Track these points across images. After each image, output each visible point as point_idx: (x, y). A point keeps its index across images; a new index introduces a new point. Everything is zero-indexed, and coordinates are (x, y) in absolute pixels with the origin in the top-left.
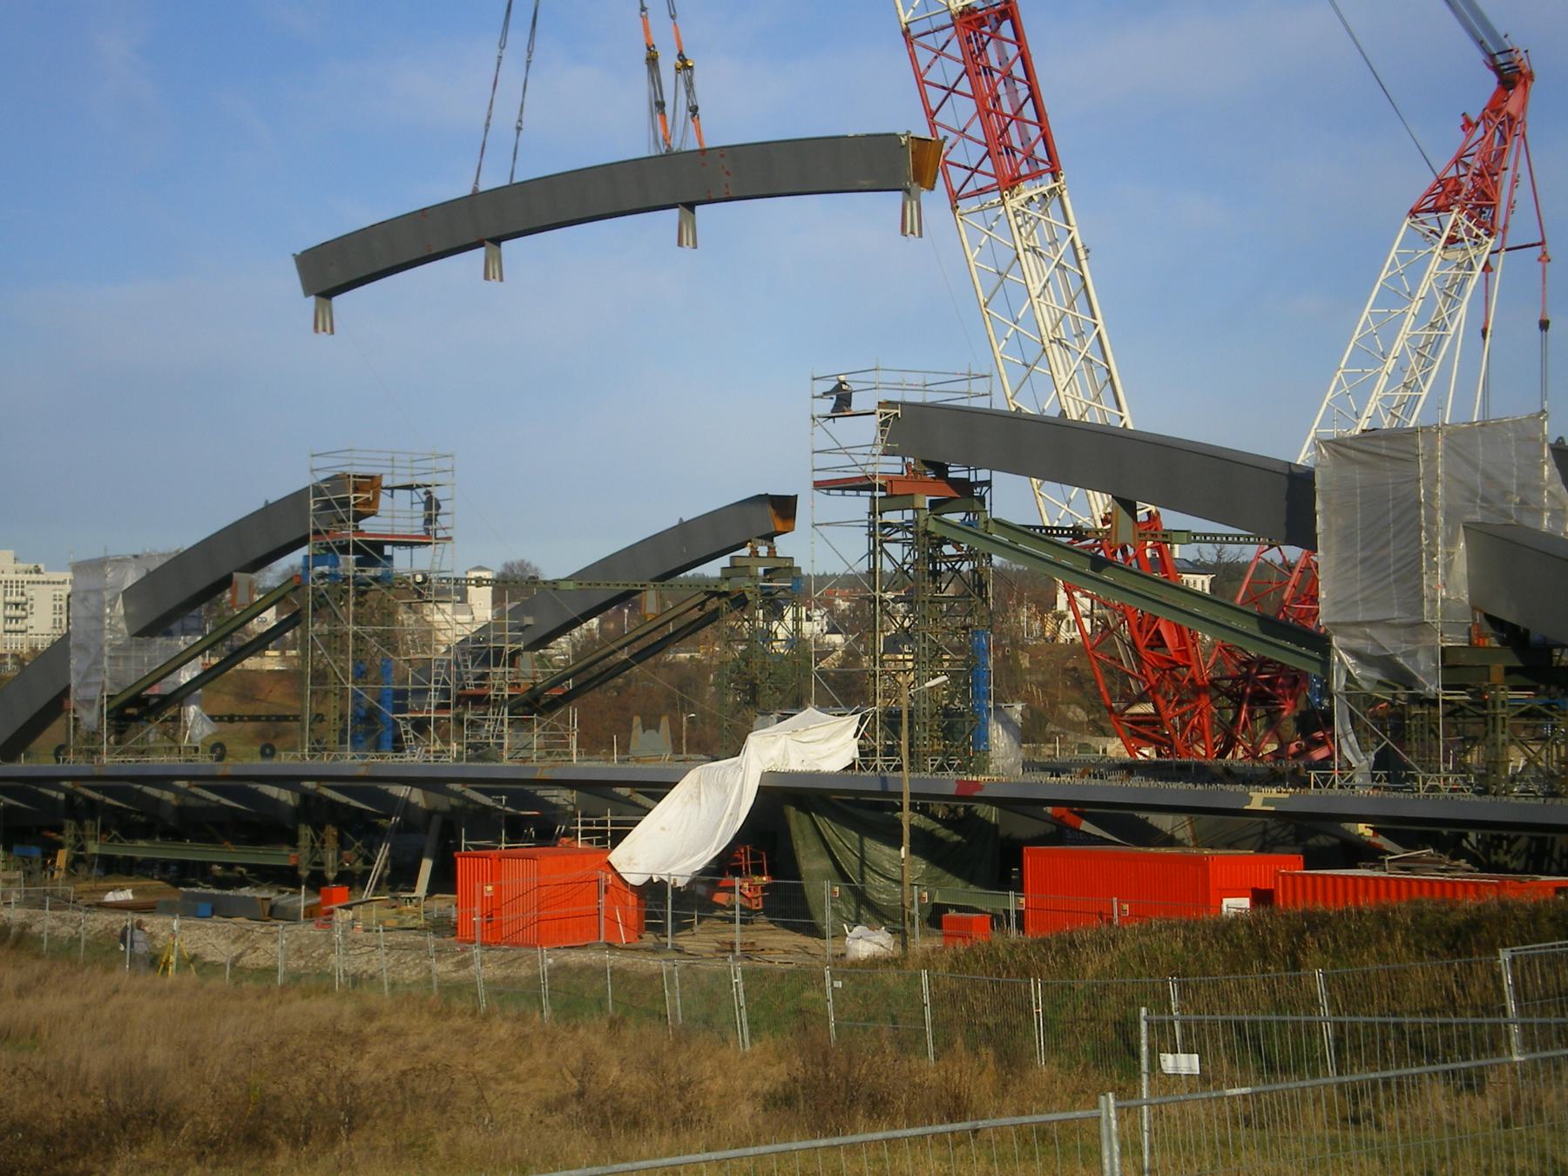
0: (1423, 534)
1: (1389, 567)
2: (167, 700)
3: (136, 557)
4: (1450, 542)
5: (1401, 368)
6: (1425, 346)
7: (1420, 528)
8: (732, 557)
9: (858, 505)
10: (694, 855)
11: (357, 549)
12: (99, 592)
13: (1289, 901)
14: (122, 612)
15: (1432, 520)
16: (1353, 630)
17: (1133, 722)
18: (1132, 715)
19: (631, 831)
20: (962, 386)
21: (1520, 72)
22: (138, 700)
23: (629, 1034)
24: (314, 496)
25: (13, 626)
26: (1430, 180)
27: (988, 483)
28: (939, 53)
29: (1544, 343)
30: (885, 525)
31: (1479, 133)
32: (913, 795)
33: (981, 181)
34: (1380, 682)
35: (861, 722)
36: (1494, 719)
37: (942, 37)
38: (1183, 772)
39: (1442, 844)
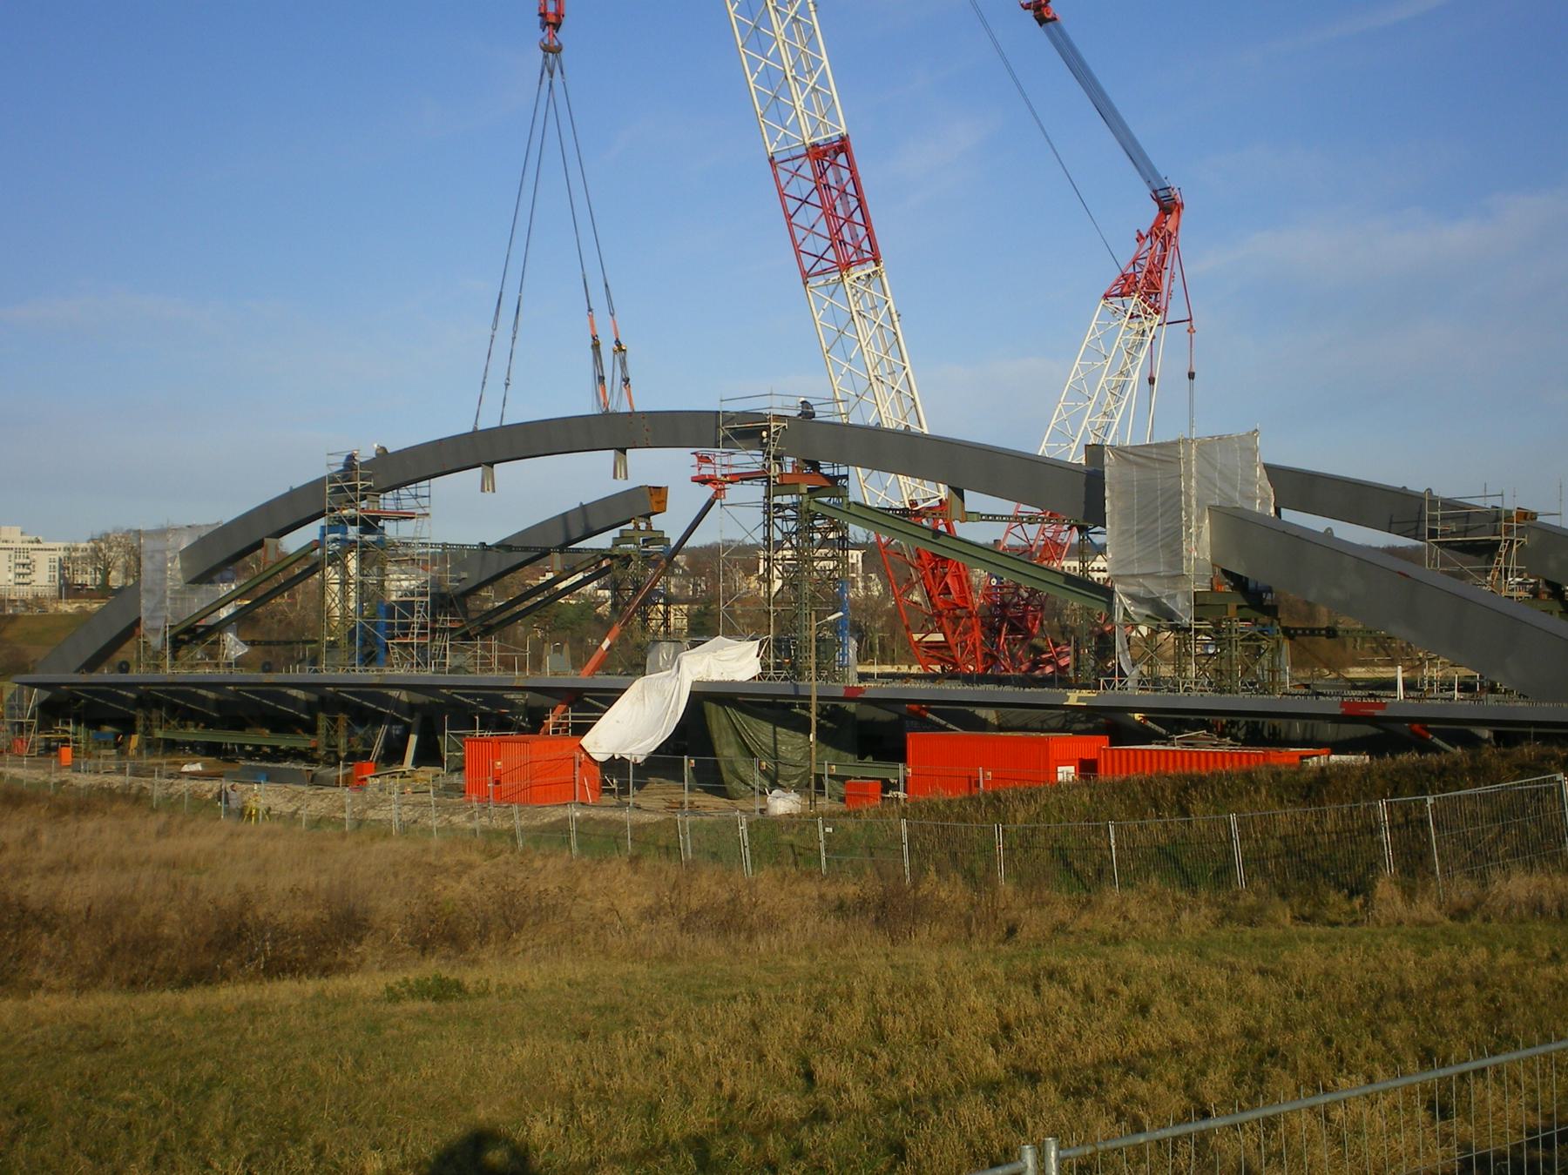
0: (1183, 513)
2: (210, 629)
3: (189, 527)
4: (1200, 519)
5: (1100, 404)
6: (1115, 388)
7: (1181, 509)
8: (621, 531)
9: (756, 491)
10: (642, 741)
11: (363, 521)
12: (163, 552)
13: (1170, 765)
14: (179, 566)
15: (1189, 505)
16: (1130, 580)
17: (926, 647)
18: (927, 642)
19: (594, 724)
20: (829, 408)
21: (1175, 203)
23: (646, 864)
24: (330, 483)
25: (21, 580)
26: (1120, 274)
27: (846, 477)
28: (795, 174)
29: (1191, 388)
30: (776, 506)
31: (1147, 244)
32: (819, 698)
33: (825, 264)
34: (1147, 616)
35: (760, 648)
37: (798, 162)
38: (968, 679)
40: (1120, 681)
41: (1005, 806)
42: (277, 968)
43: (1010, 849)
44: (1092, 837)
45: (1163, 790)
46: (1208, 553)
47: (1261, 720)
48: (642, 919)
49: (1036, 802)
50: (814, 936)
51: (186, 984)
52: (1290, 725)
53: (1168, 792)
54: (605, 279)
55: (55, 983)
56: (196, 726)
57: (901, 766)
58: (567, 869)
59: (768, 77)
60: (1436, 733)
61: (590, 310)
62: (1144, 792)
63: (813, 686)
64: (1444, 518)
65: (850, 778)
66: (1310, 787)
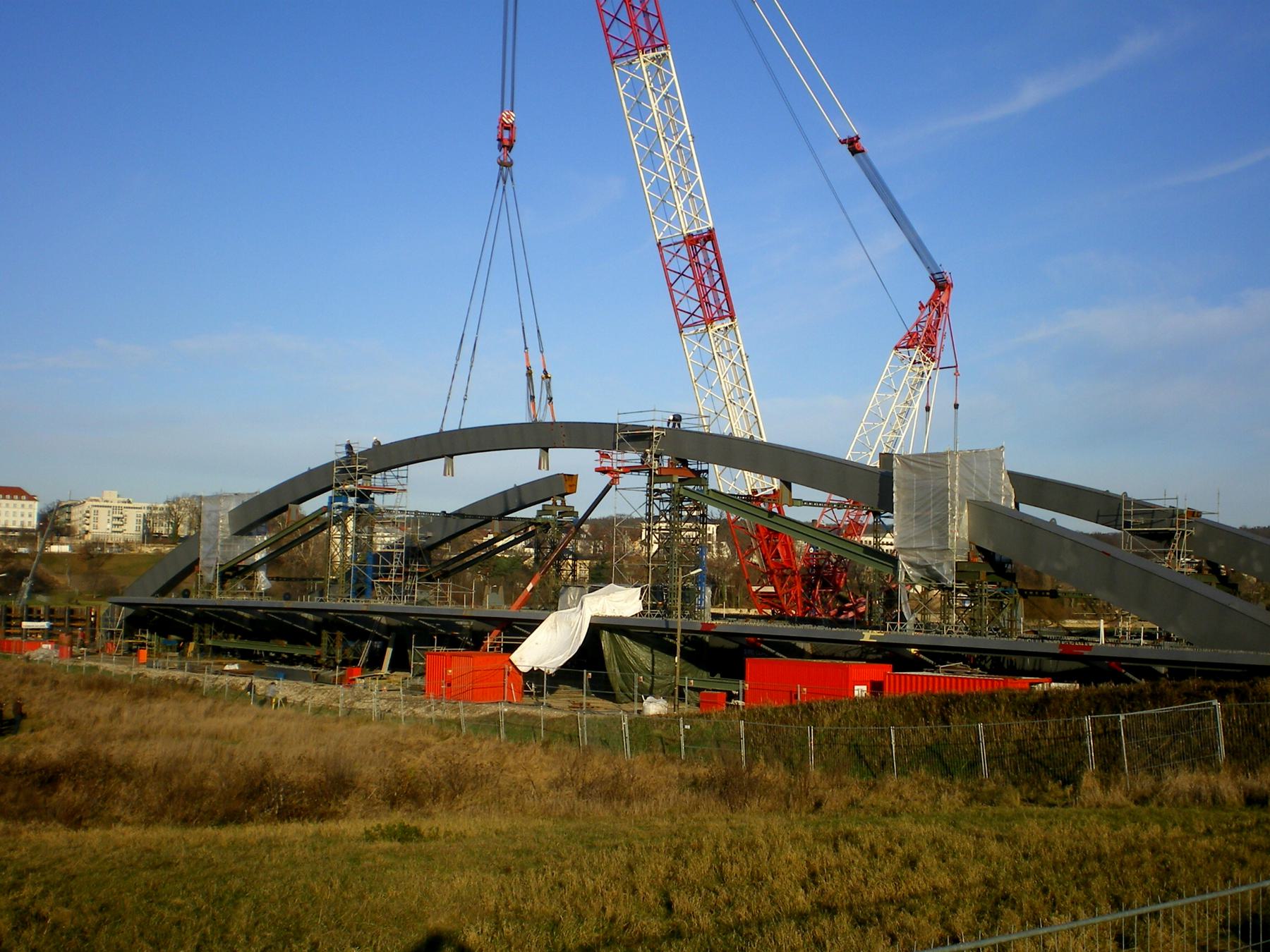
1: (929, 521)
3: (236, 494)
4: (961, 509)
5: (890, 424)
7: (948, 502)
8: (544, 505)
9: (642, 480)
12: (217, 512)
13: (936, 687)
15: (953, 499)
16: (910, 552)
17: (762, 596)
18: (762, 593)
19: (520, 645)
22: (230, 569)
23: (554, 748)
25: (116, 529)
26: (906, 332)
27: (707, 471)
28: (675, 255)
29: (956, 414)
30: (655, 490)
31: (927, 311)
32: (683, 631)
33: (695, 319)
35: (642, 594)
36: (981, 598)
37: (679, 246)
38: (792, 620)
39: (965, 660)
40: (901, 625)
41: (816, 713)
42: (286, 814)
43: (818, 745)
44: (879, 738)
45: (930, 704)
46: (966, 534)
47: (1002, 656)
48: (551, 787)
49: (838, 711)
50: (675, 804)
51: (222, 822)
52: (1024, 661)
53: (934, 707)
54: (538, 327)
55: (129, 818)
56: (235, 638)
57: (741, 682)
58: (496, 749)
59: (658, 186)
60: (1128, 669)
61: (526, 348)
62: (917, 705)
63: (678, 622)
64: (1135, 514)
65: (704, 689)
66: (1036, 705)
